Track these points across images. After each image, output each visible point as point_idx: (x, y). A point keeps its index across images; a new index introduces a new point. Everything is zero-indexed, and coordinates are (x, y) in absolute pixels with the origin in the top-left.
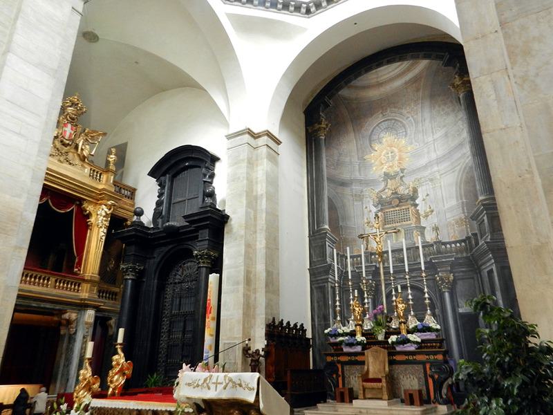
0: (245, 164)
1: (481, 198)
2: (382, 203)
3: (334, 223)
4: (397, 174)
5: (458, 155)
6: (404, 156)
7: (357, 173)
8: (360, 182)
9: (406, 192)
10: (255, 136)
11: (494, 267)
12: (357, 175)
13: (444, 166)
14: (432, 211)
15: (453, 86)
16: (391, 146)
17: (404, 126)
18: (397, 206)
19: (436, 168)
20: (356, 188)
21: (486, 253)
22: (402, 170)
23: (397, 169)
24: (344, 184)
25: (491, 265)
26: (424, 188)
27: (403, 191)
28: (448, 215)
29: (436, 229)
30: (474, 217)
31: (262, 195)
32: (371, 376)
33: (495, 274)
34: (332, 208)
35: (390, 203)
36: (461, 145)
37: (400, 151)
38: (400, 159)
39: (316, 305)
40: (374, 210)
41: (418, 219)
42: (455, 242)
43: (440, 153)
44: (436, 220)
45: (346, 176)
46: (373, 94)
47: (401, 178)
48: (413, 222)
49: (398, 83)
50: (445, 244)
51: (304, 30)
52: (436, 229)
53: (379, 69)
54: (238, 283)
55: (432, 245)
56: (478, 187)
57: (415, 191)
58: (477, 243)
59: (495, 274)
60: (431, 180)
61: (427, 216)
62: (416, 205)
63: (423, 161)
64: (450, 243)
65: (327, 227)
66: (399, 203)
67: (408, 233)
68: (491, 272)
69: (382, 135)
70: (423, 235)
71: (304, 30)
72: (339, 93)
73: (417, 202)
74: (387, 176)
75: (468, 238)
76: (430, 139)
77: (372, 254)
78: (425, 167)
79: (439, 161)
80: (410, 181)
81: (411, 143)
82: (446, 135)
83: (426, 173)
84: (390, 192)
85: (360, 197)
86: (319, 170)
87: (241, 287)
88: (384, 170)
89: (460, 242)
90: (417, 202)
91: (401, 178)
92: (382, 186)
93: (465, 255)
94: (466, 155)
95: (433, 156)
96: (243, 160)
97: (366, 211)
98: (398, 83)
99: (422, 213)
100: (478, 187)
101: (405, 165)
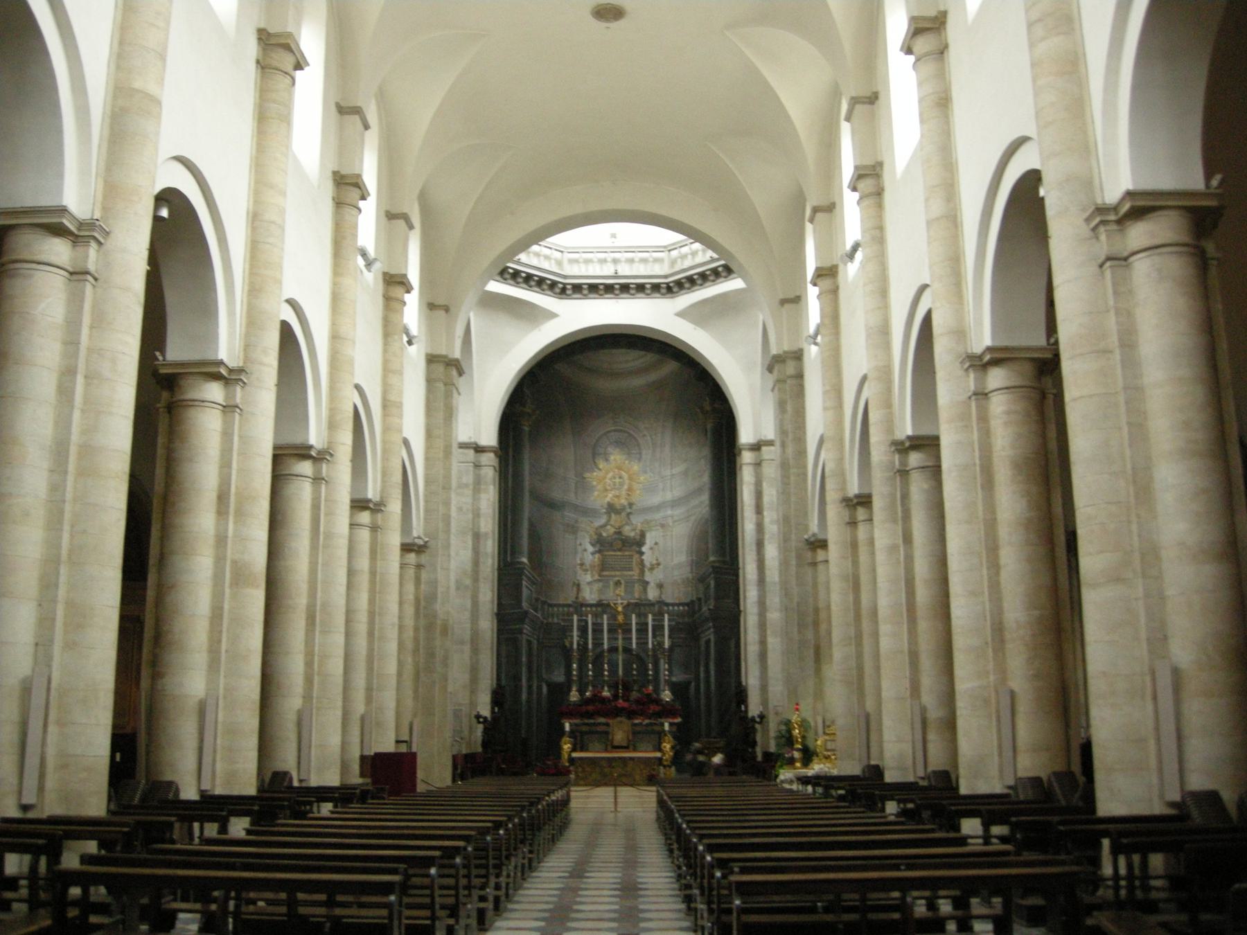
0: (469, 492)
1: (712, 559)
2: (602, 544)
3: (538, 561)
4: (623, 509)
5: (695, 502)
6: (635, 486)
7: (572, 495)
8: (576, 508)
9: (632, 534)
10: (479, 449)
11: (712, 638)
12: (571, 497)
13: (678, 512)
14: (658, 564)
15: (701, 408)
16: (620, 468)
17: (638, 445)
18: (620, 550)
19: (669, 512)
20: (569, 515)
21: (707, 620)
22: (631, 505)
23: (623, 501)
24: (553, 505)
25: (710, 635)
26: (654, 533)
27: (628, 531)
28: (676, 573)
29: (660, 586)
30: (702, 579)
31: (486, 534)
32: (616, 743)
33: (712, 645)
34: (534, 535)
35: (611, 544)
36: (699, 491)
37: (630, 479)
38: (630, 489)
39: (504, 660)
40: (591, 549)
41: (642, 572)
42: (679, 605)
43: (678, 492)
44: (661, 576)
45: (557, 495)
46: (606, 386)
47: (629, 514)
48: (635, 573)
49: (638, 382)
50: (667, 605)
51: (552, 315)
52: (660, 586)
53: (614, 351)
54: (462, 643)
55: (653, 605)
56: (710, 546)
57: (643, 535)
58: (700, 609)
59: (712, 645)
60: (663, 526)
61: (652, 569)
62: (642, 553)
63: (656, 500)
64: (673, 605)
65: (525, 560)
66: (621, 547)
67: (630, 584)
68: (708, 642)
69: (610, 449)
70: (645, 590)
71: (552, 315)
72: (556, 367)
73: (644, 549)
74: (611, 509)
75: (692, 602)
76: (668, 472)
77: (582, 605)
78: (658, 508)
79: (674, 504)
80: (637, 520)
81: (645, 472)
82: (685, 473)
83: (658, 516)
84: (612, 530)
85: (573, 529)
86: (518, 475)
87: (467, 648)
88: (608, 499)
89: (687, 604)
90: (644, 549)
91: (629, 514)
92: (603, 520)
93: (686, 620)
94: (702, 504)
95: (669, 496)
96: (466, 486)
97: (580, 549)
98: (638, 382)
99: (647, 564)
100: (710, 546)
101: (633, 500)
